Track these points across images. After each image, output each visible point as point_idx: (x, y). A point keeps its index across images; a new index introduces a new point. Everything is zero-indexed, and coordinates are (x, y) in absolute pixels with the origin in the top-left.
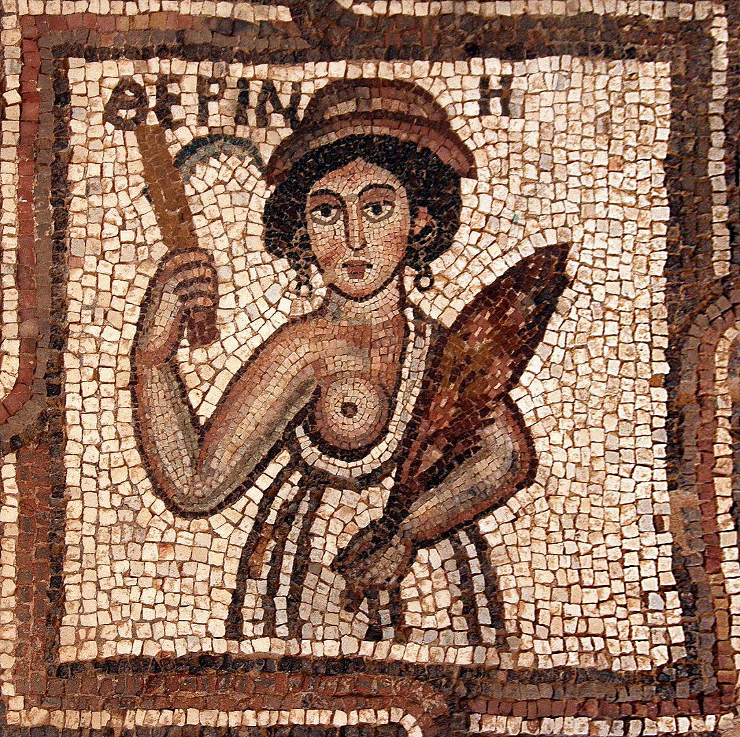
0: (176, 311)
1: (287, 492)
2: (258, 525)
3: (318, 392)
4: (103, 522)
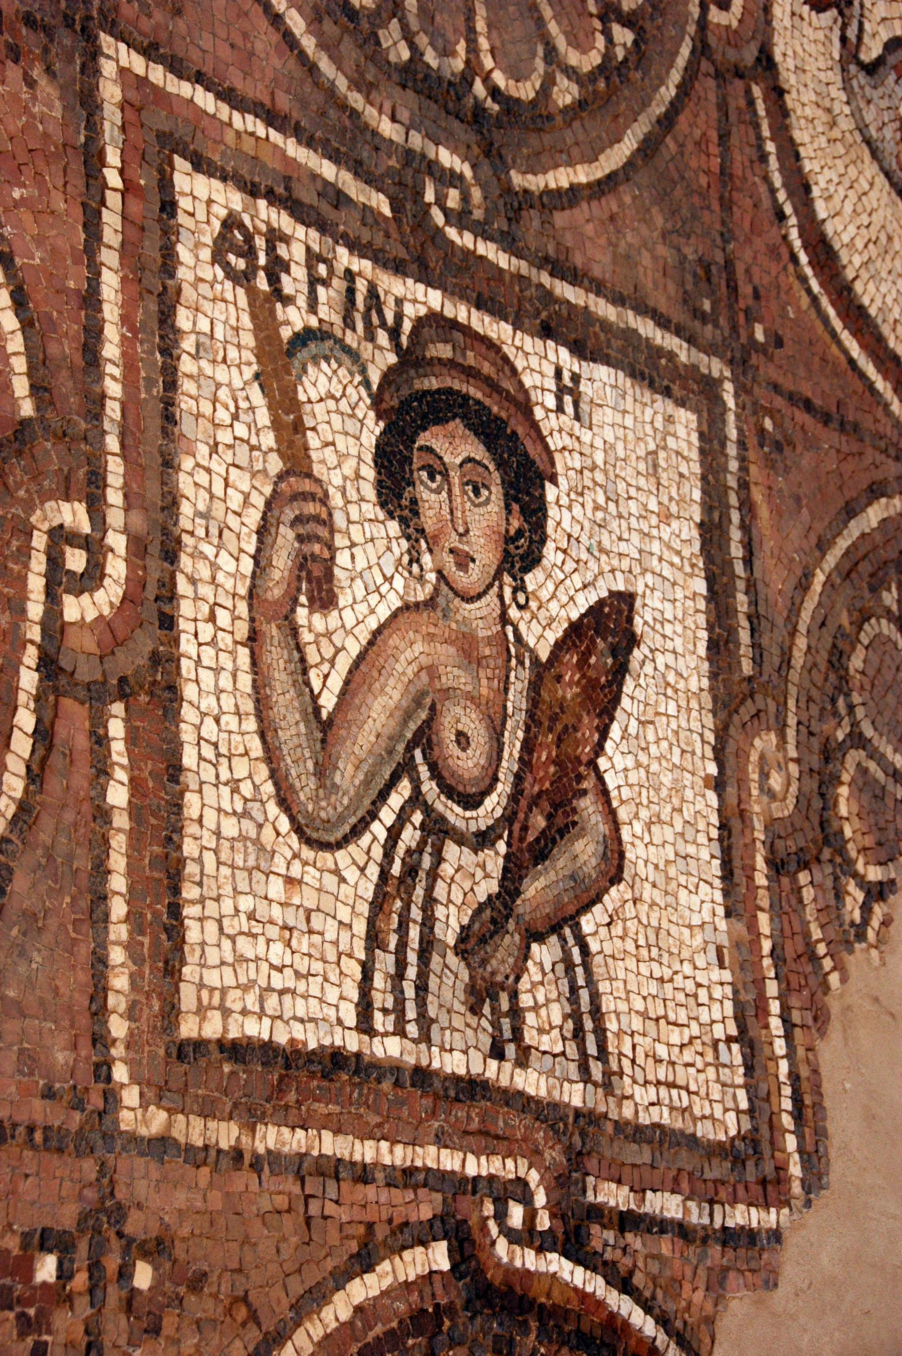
0: (294, 553)
1: (409, 836)
2: (384, 875)
3: (433, 708)
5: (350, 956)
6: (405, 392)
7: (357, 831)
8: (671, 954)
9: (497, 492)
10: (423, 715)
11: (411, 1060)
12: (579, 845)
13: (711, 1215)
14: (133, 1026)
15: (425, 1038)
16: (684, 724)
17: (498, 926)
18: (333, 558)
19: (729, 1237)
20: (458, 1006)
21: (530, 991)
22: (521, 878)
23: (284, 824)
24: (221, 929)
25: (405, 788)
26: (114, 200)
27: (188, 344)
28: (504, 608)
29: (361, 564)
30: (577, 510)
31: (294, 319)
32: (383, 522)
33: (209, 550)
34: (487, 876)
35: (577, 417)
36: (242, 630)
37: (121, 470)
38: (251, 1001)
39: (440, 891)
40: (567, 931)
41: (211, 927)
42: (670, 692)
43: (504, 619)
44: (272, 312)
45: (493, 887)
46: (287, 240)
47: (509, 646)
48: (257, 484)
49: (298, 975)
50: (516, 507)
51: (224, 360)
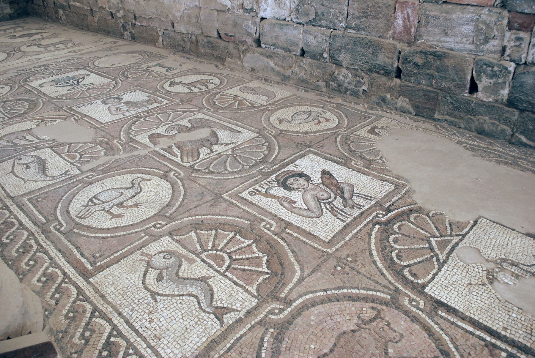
1: (328, 206)
2: (330, 211)
9: (300, 179)
19: (405, 194)
25: (322, 204)
31: (264, 191)
36: (290, 213)
38: (330, 232)
39: (337, 206)
43: (313, 184)
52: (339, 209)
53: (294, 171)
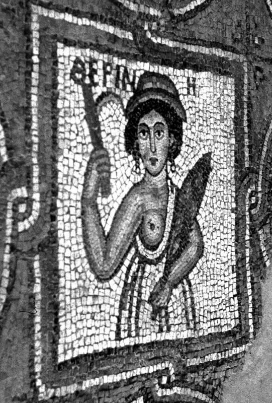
1: (134, 268)
2: (126, 284)
3: (143, 219)
4: (73, 288)
5: (113, 316)
6: (136, 105)
7: (116, 272)
8: (217, 275)
10: (139, 222)
11: (132, 344)
12: (190, 250)
13: (225, 355)
14: (43, 365)
15: (137, 335)
16: (225, 193)
17: (162, 289)
18: (110, 176)
20: (148, 320)
21: (172, 306)
22: (170, 268)
23: (92, 277)
24: (72, 322)
25: (133, 250)
26: (36, 68)
27: (61, 114)
28: (167, 173)
29: (119, 175)
30: (193, 130)
31: (98, 91)
32: (127, 157)
33: (67, 188)
34: (159, 272)
35: (194, 94)
36: (79, 212)
37: (38, 170)
40: (185, 281)
41: (69, 322)
42: (221, 183)
43: (168, 178)
44: (91, 91)
45: (161, 275)
46: (96, 61)
47: (169, 186)
48: (84, 158)
49: (96, 328)
50: (172, 135)
51: (74, 115)
52: (140, 293)
53: (176, 96)
